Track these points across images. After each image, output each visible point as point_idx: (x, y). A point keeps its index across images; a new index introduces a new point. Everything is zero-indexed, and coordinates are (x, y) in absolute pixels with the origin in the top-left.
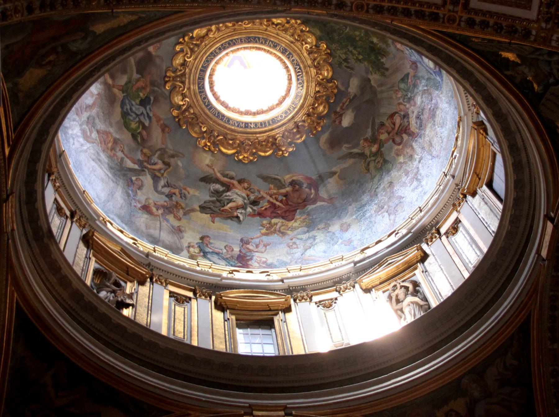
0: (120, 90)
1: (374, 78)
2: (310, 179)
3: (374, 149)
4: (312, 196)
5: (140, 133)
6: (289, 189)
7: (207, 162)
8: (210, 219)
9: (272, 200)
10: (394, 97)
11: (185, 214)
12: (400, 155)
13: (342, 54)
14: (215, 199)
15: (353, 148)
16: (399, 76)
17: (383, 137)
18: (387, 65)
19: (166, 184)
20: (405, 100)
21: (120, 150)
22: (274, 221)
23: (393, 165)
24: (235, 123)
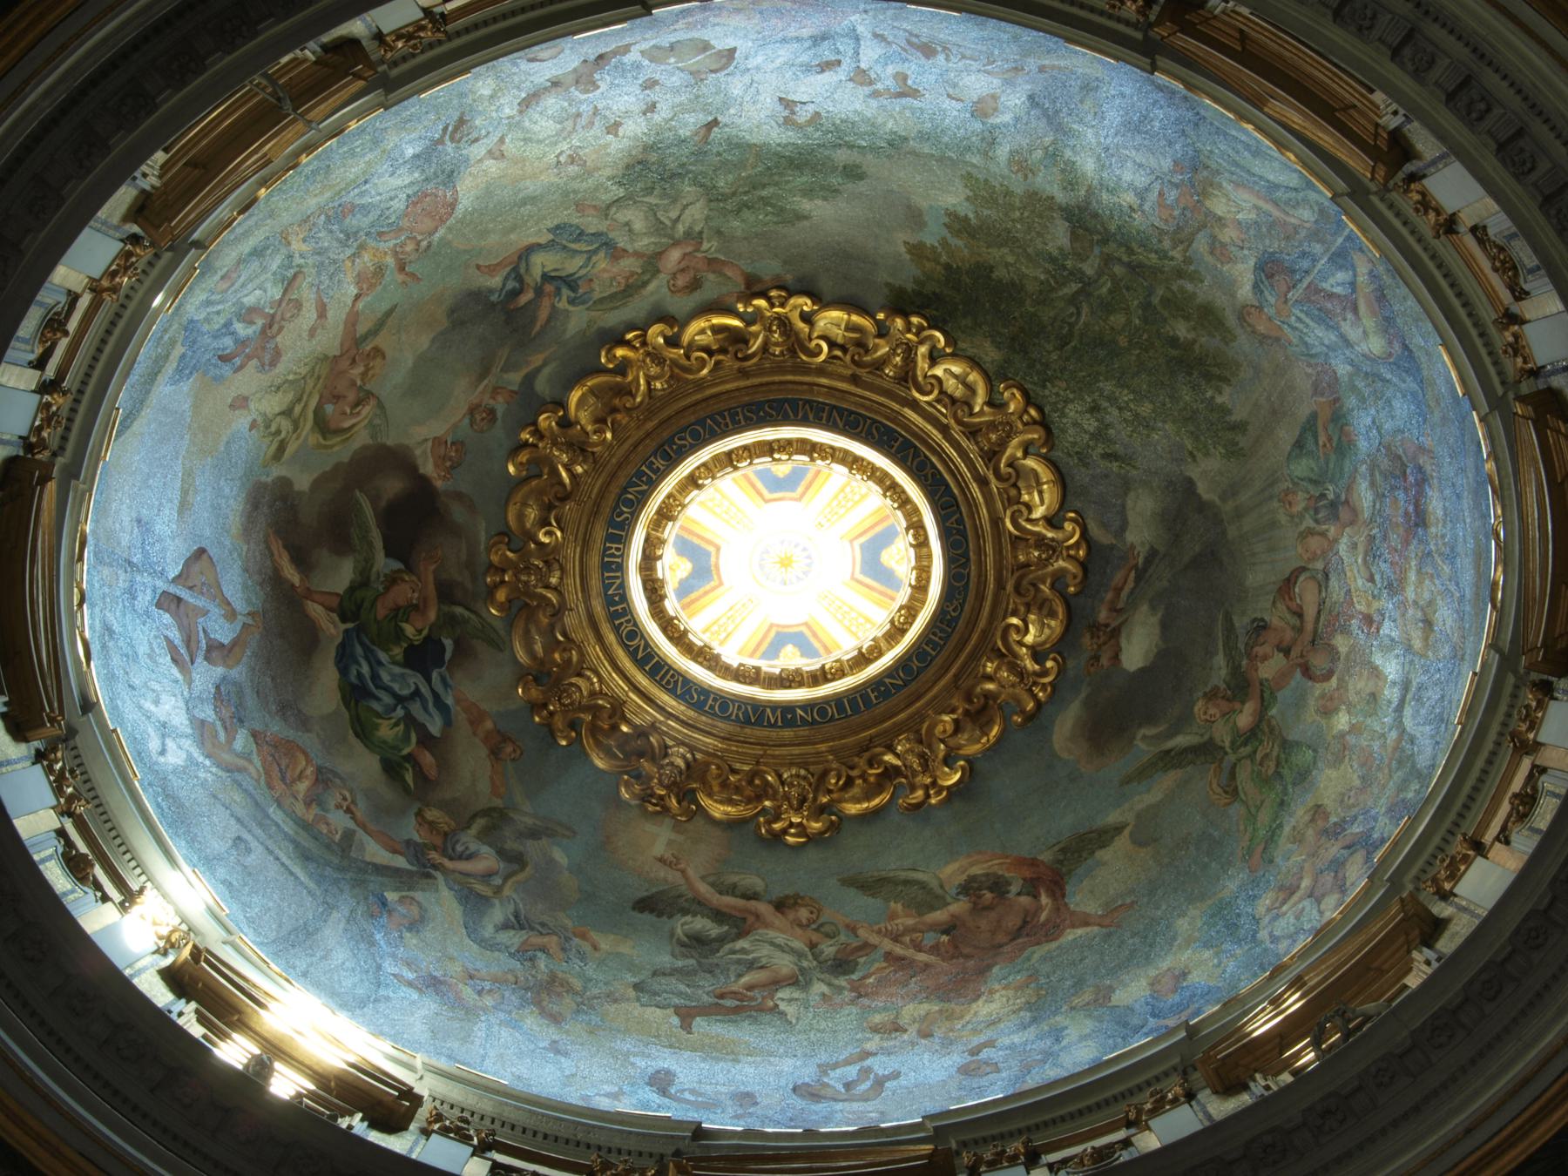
0: (329, 609)
2: (1034, 863)
3: (1244, 719)
4: (1043, 917)
5: (410, 758)
6: (959, 907)
7: (659, 849)
8: (675, 1020)
9: (898, 950)
10: (1283, 519)
12: (1336, 710)
16: (1285, 436)
19: (512, 918)
20: (1320, 516)
21: (338, 807)
23: (1315, 751)
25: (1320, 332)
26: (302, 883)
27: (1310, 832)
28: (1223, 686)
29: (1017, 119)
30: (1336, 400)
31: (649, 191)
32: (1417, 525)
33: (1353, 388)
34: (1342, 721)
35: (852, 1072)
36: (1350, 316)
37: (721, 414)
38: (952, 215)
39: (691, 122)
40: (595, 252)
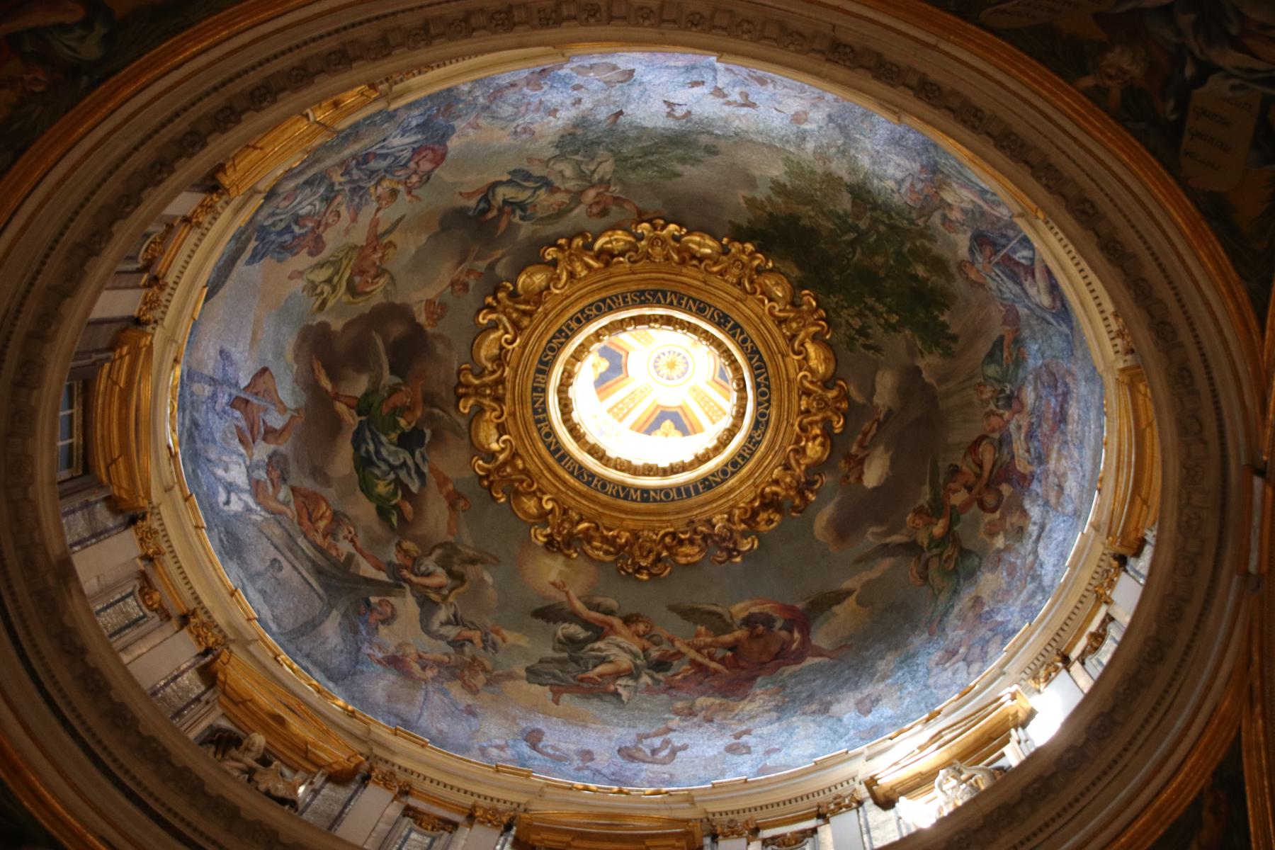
0: (350, 407)
1: (929, 363)
2: (791, 609)
3: (938, 529)
5: (396, 507)
6: (740, 634)
7: (553, 576)
8: (550, 695)
9: (699, 659)
10: (976, 402)
11: (489, 683)
13: (852, 316)
14: (565, 655)
15: (890, 533)
16: (983, 348)
17: (958, 498)
18: (952, 331)
19: (452, 618)
21: (345, 538)
22: (702, 701)
23: (981, 559)
24: (618, 492)
25: (1010, 285)
26: (314, 590)
27: (970, 614)
28: (926, 506)
29: (821, 127)
30: (1017, 330)
31: (576, 152)
32: (1060, 422)
33: (1029, 324)
34: (1000, 542)
35: (657, 742)
36: (1030, 278)
37: (617, 296)
38: (773, 181)
39: (603, 114)
40: (539, 188)
